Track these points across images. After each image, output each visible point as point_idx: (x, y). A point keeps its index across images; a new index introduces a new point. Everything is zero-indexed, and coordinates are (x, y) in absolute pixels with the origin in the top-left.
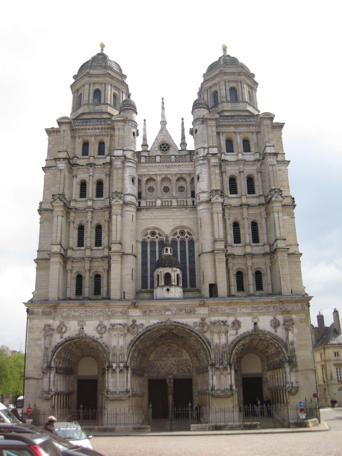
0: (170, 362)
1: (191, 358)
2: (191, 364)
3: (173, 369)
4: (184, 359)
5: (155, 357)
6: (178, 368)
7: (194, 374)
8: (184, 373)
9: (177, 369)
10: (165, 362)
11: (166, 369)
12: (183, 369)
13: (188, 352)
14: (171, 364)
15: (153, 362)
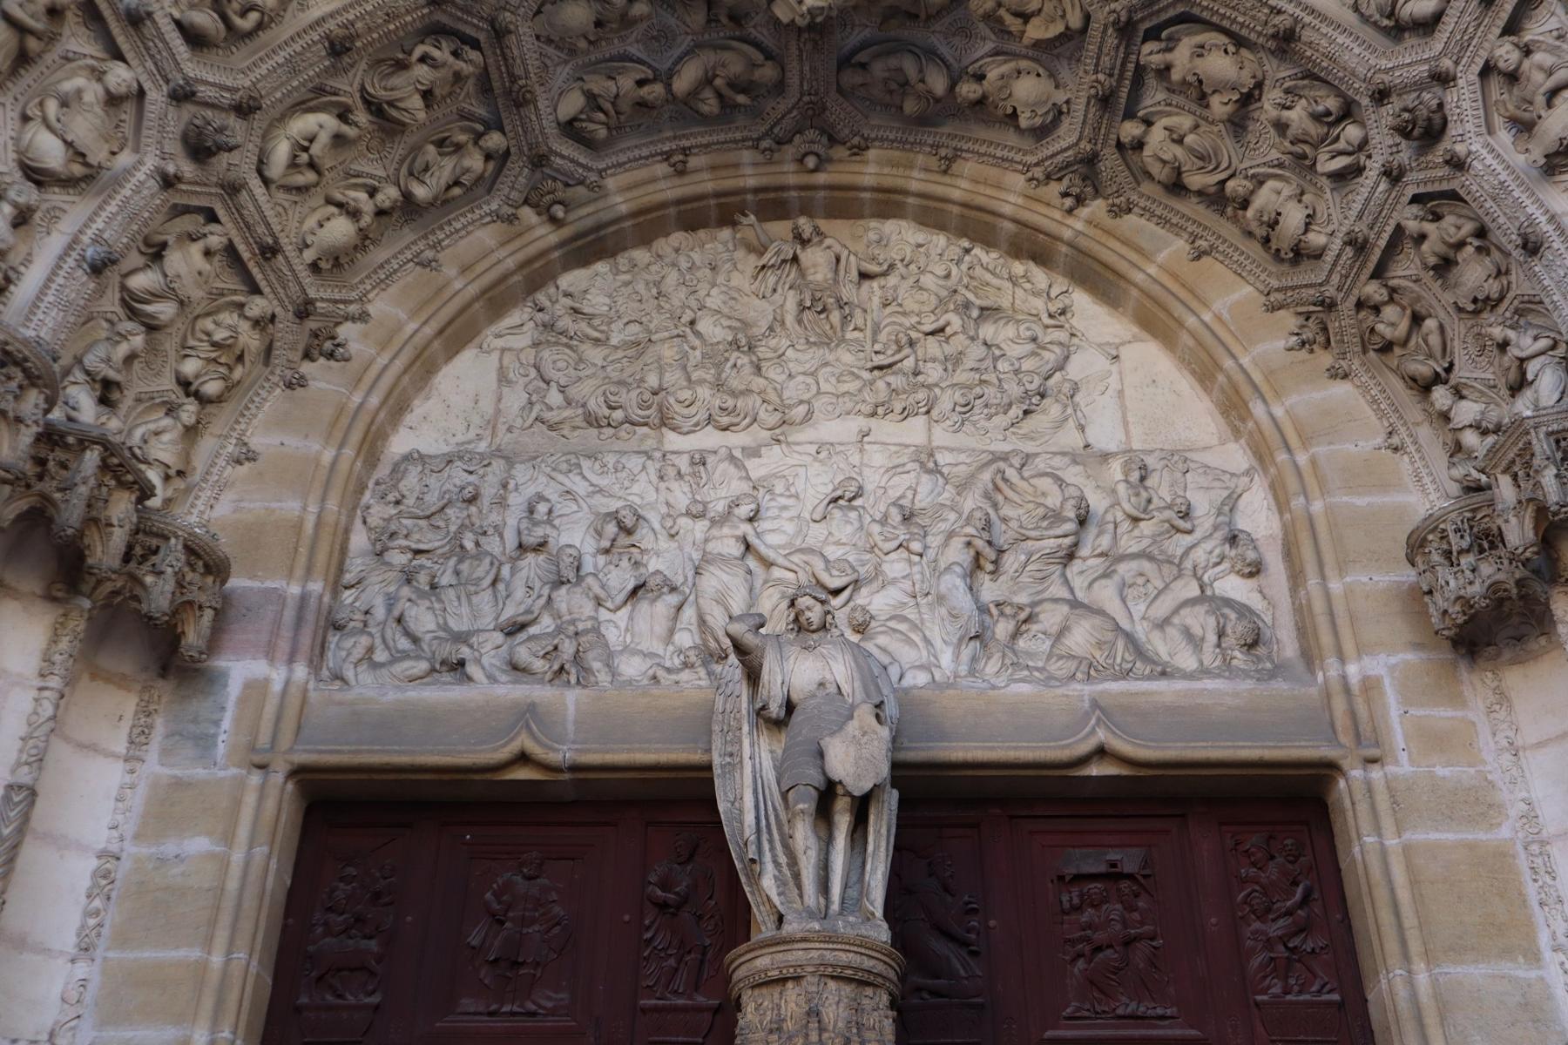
0: (817, 484)
1: (1233, 408)
2: (1258, 516)
3: (878, 601)
4: (1105, 434)
5: (515, 400)
6: (990, 590)
7: (1384, 666)
8: (1126, 674)
9: (963, 600)
10: (724, 487)
11: (712, 581)
12: (1106, 595)
13: (1156, 321)
14: (842, 499)
15: (457, 475)
